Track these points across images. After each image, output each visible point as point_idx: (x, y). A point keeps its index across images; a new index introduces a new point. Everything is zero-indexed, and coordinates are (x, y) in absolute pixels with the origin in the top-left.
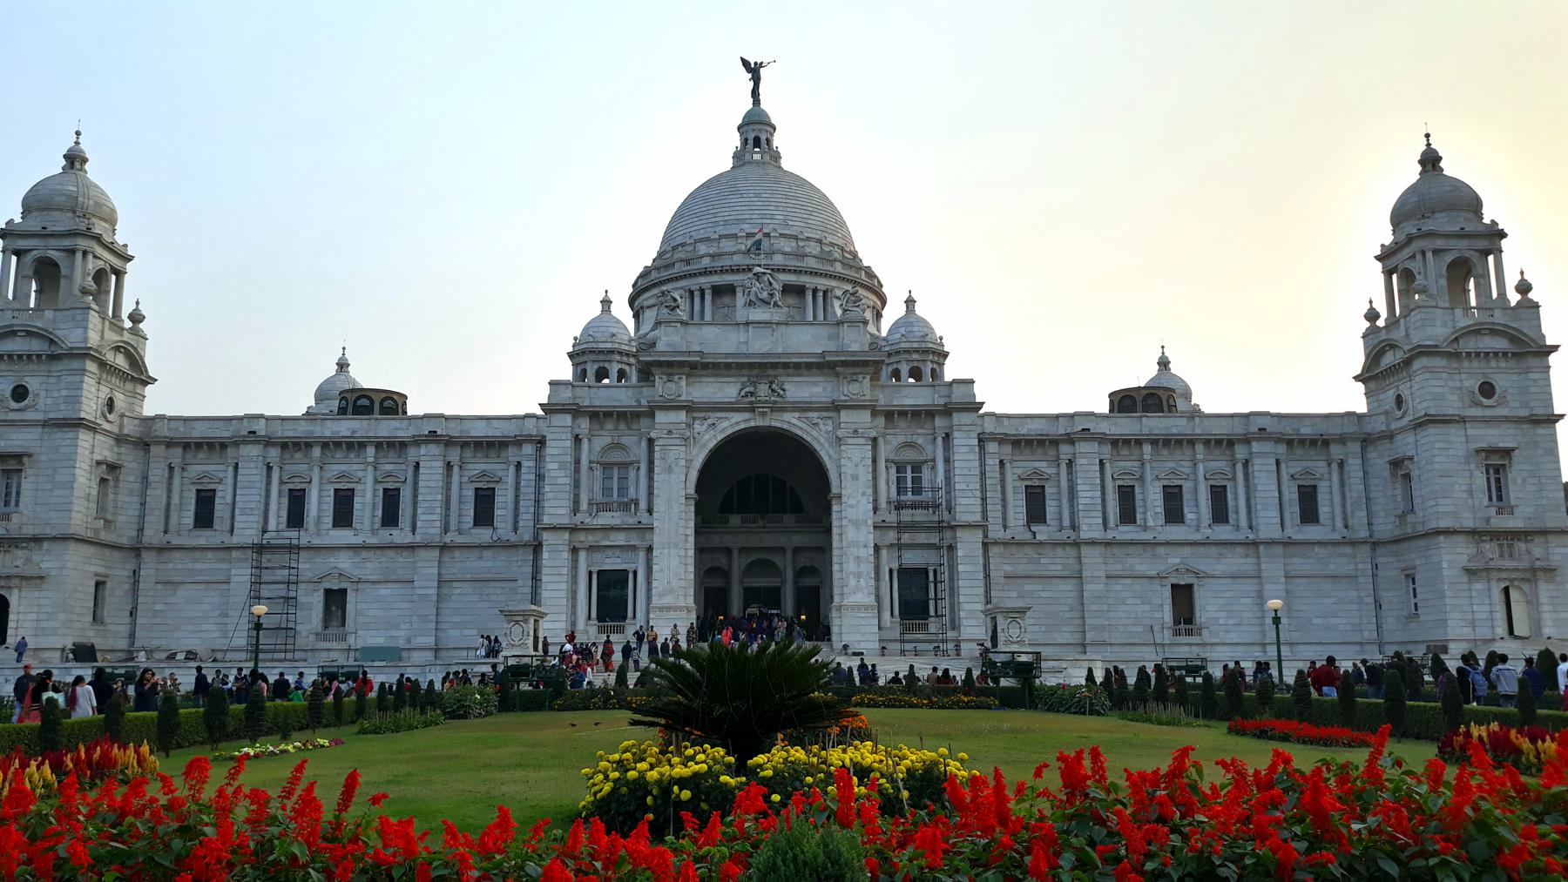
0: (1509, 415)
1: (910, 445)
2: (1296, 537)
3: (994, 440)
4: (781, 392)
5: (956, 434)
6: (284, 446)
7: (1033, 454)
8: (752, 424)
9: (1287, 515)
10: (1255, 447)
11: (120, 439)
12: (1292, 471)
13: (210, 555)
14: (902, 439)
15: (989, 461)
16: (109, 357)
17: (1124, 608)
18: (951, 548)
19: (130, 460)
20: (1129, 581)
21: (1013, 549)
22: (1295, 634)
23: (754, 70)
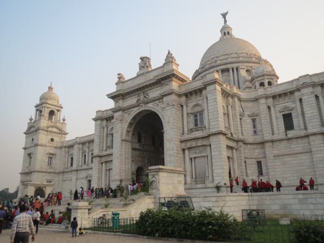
1: (197, 105)
4: (147, 96)
5: (208, 96)
6: (82, 144)
7: (285, 100)
8: (140, 110)
11: (56, 148)
13: (70, 173)
14: (195, 103)
16: (50, 129)
18: (210, 145)
19: (58, 152)
21: (278, 143)
23: (224, 15)
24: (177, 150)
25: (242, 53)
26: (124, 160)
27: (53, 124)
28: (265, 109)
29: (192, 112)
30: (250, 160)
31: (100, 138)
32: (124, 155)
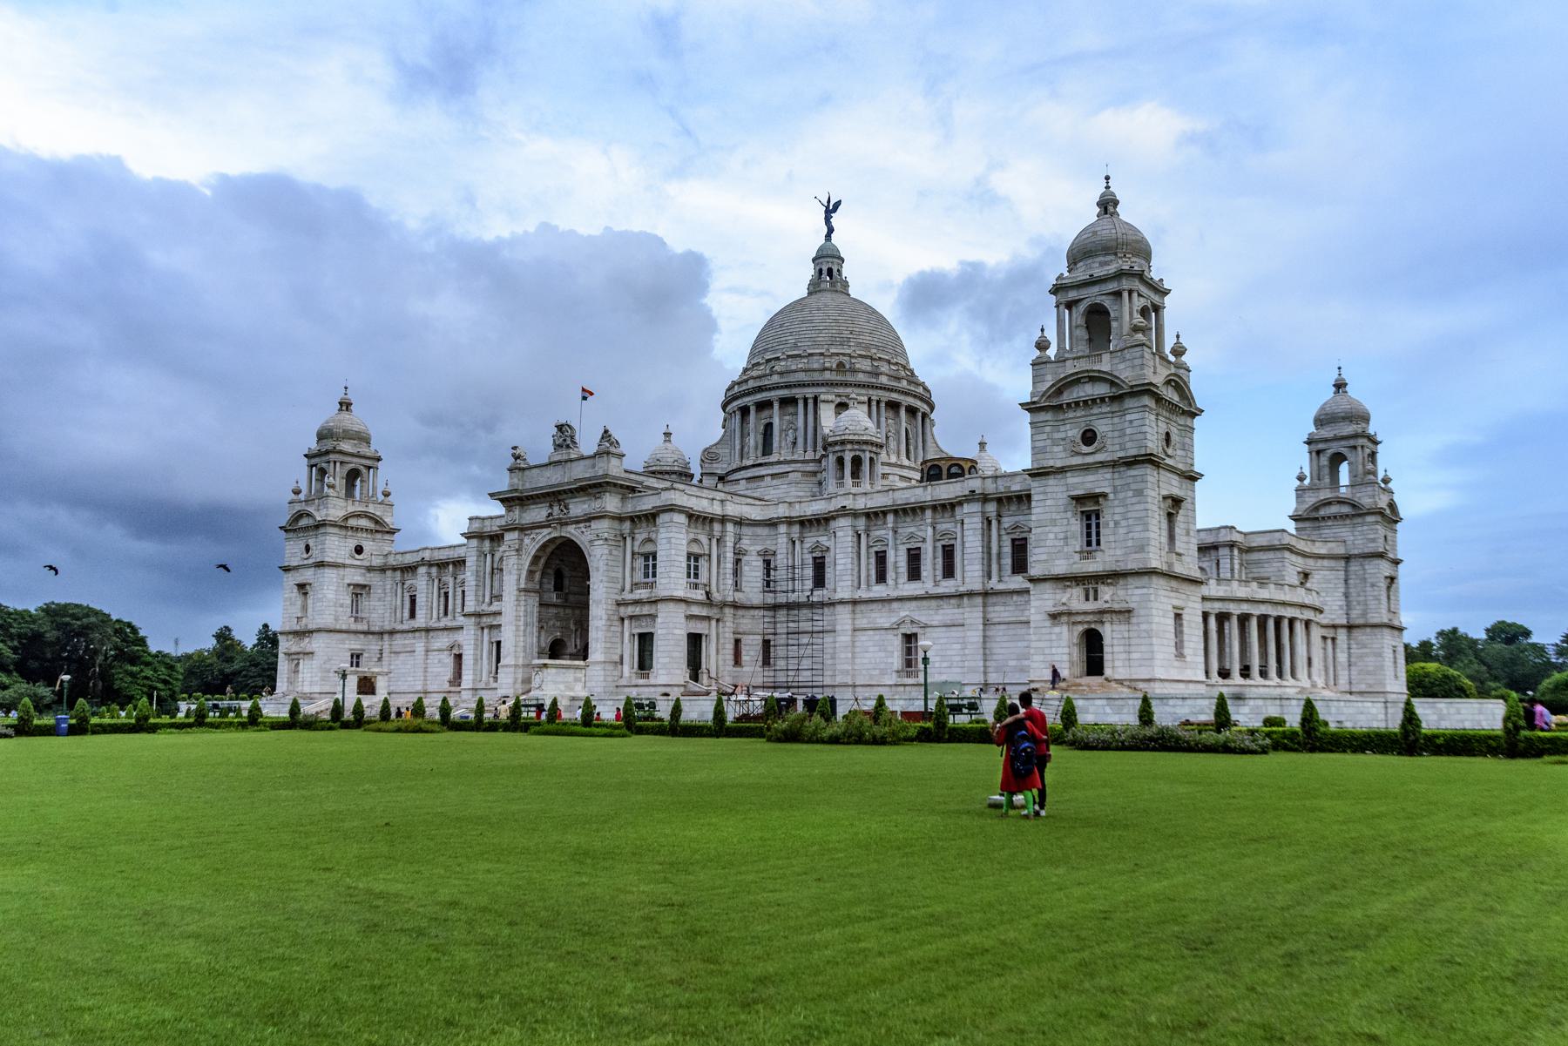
0: (1109, 459)
1: (649, 540)
2: (1001, 587)
3: (783, 522)
7: (818, 530)
8: (553, 535)
9: (995, 567)
10: (967, 508)
11: (370, 569)
12: (1006, 526)
13: (410, 635)
14: (645, 536)
15: (780, 541)
16: (352, 522)
17: (867, 655)
19: (374, 579)
20: (871, 632)
22: (994, 675)
24: (609, 619)
25: (838, 354)
26: (522, 628)
27: (359, 508)
28: (784, 546)
29: (642, 551)
30: (751, 637)
31: (477, 576)
32: (522, 619)
